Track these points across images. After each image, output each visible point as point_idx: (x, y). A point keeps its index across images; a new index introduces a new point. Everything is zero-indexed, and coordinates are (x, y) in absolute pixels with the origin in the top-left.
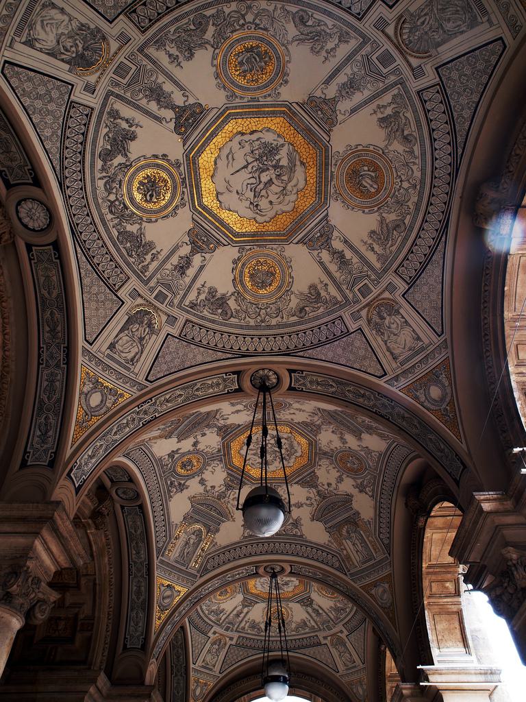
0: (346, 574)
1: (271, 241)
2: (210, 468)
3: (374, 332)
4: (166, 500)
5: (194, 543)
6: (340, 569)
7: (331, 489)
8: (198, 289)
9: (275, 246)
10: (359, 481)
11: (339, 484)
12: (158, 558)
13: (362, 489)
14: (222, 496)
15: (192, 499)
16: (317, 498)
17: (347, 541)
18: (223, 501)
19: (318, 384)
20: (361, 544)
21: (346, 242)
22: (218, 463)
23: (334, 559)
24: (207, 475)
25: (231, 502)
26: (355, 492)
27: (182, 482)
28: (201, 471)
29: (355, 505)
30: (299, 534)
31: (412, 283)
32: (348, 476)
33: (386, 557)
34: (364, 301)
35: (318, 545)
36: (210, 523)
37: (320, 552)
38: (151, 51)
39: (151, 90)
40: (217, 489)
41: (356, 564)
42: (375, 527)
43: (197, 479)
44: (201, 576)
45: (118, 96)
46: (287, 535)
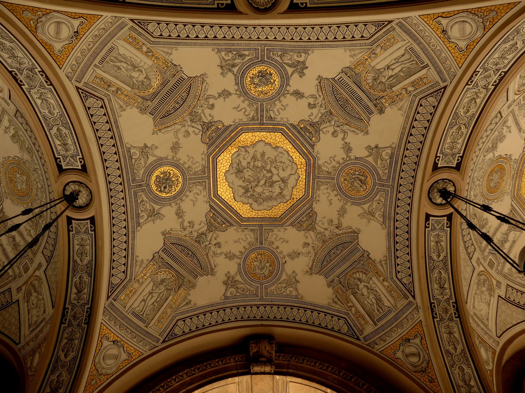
0: (108, 298)
1: (515, 184)
2: (245, 105)
3: (476, 281)
4: (219, 45)
5: (131, 77)
6: (112, 288)
7: (213, 248)
8: (511, 127)
9: (511, 188)
10: (238, 278)
11: (223, 256)
12: (132, 20)
13: (230, 282)
14: (194, 117)
15: (203, 77)
16: (195, 234)
17: (152, 284)
18: (187, 118)
19: (437, 242)
20: (156, 301)
21: (514, 242)
22: (251, 116)
23: (122, 276)
24: (235, 100)
25: (184, 129)
26: (221, 276)
27: (235, 70)
28: (243, 92)
29: (202, 280)
30: (141, 221)
31: (507, 300)
32: (239, 264)
33: (159, 340)
34: (486, 265)
35: (133, 249)
36: (156, 101)
37: (124, 253)
40: (207, 112)
41: (128, 306)
42: (188, 312)
43: (232, 87)
44: (77, 88)
46: (137, 205)
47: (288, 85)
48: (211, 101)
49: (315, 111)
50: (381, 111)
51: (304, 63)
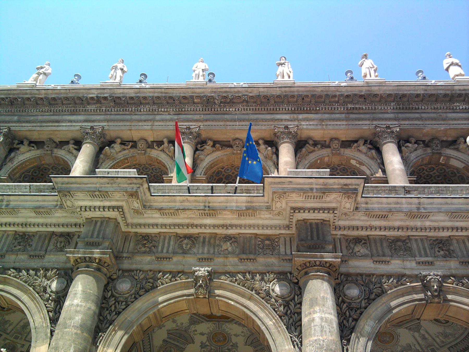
15: (246, 344)
24: (232, 332)
27: (231, 344)
38: (8, 331)
39: (23, 328)
40: (245, 331)
43: (233, 338)
45: (26, 337)
47: (207, 337)
48: (243, 334)
49: (193, 329)
50: (164, 341)
51: (202, 348)
